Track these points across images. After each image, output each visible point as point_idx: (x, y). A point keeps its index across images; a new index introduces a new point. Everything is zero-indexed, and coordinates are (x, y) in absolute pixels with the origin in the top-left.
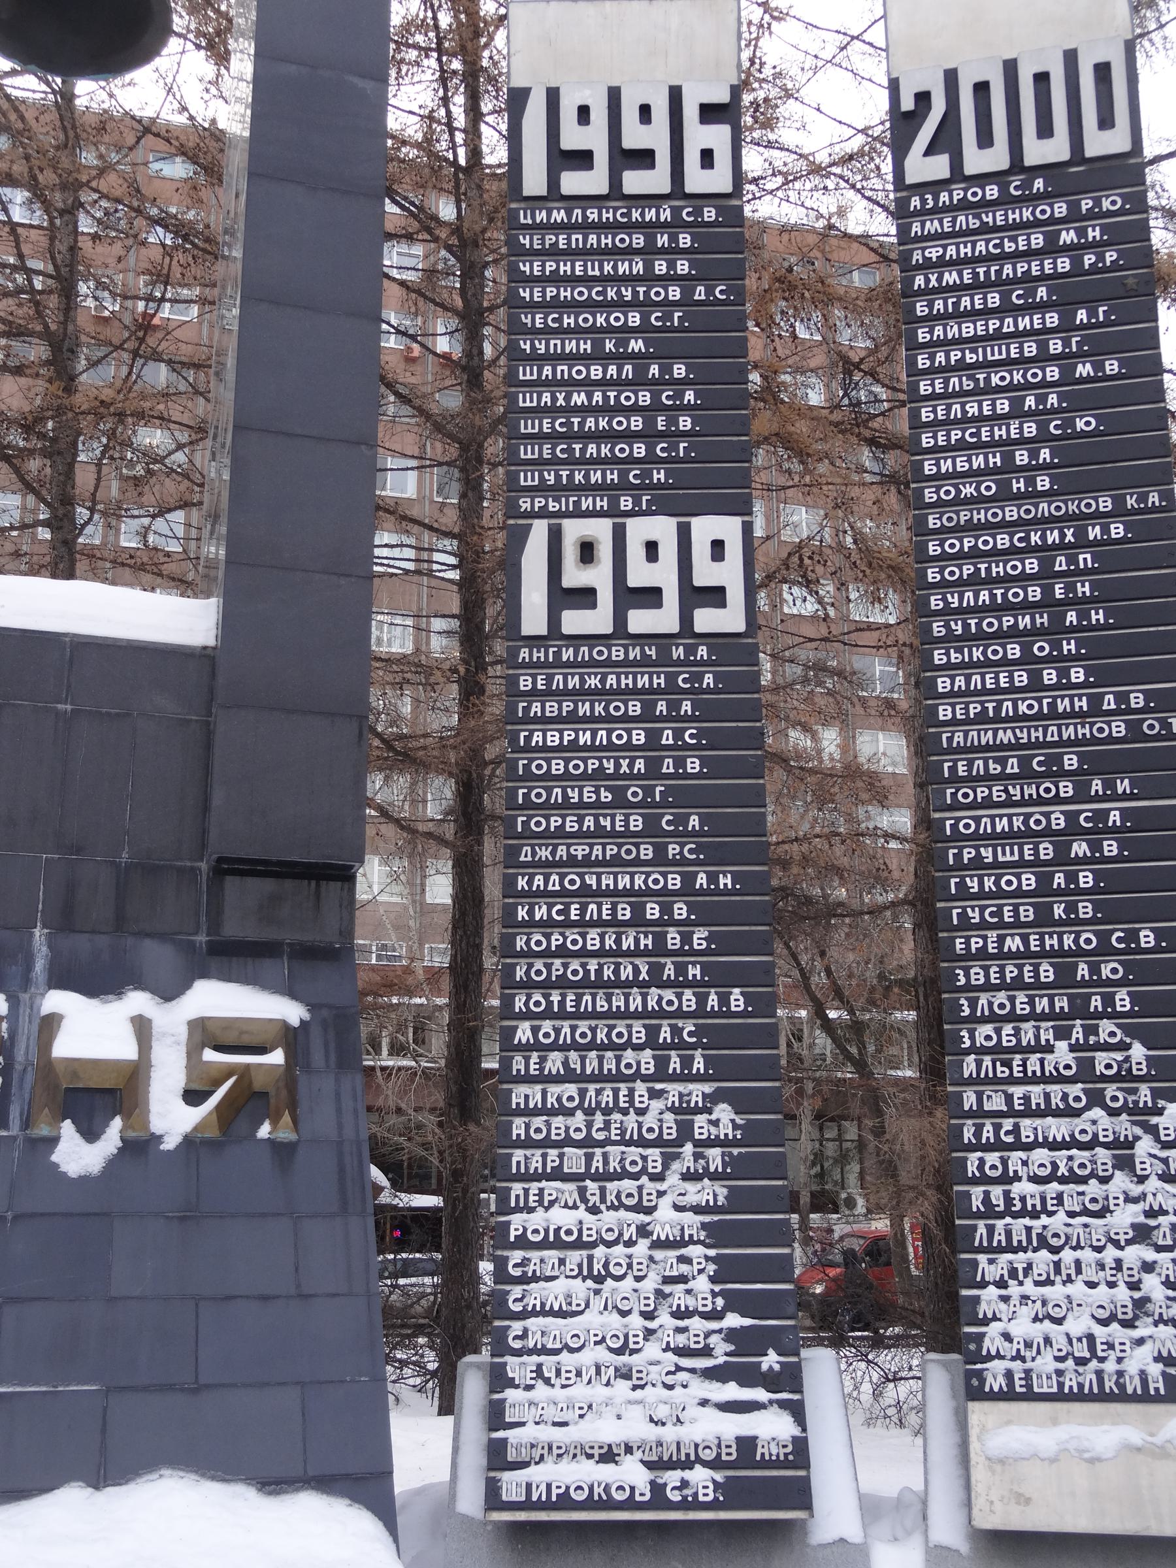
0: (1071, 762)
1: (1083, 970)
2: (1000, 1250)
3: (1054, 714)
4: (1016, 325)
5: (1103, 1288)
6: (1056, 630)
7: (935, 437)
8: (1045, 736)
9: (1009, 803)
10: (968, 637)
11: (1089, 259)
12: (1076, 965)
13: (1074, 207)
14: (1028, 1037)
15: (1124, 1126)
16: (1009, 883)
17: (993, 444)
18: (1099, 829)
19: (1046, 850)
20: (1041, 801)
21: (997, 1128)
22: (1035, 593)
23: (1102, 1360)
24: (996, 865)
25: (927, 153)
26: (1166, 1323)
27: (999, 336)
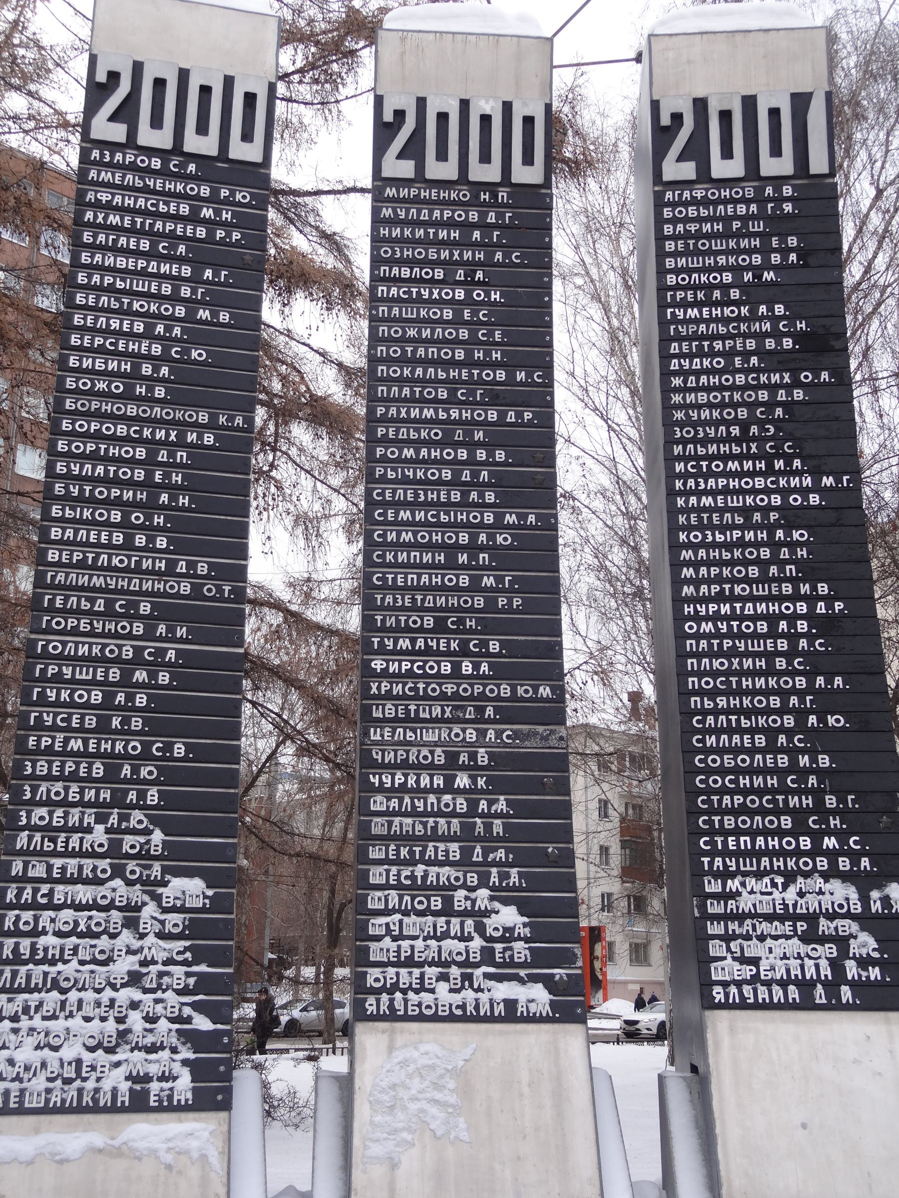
0: (145, 608)
1: (126, 770)
2: (20, 991)
3: (138, 570)
4: (159, 268)
5: (96, 1022)
6: (150, 506)
7: (82, 339)
8: (129, 585)
9: (92, 634)
10: (81, 500)
11: (220, 234)
12: (122, 765)
13: (215, 192)
14: (74, 818)
15: (136, 894)
16: (81, 697)
17: (126, 354)
18: (158, 663)
19: (115, 674)
20: (116, 636)
21: (35, 891)
22: (139, 475)
23: (85, 1080)
24: (73, 681)
25: (112, 119)
26: (140, 1050)
27: (143, 273)
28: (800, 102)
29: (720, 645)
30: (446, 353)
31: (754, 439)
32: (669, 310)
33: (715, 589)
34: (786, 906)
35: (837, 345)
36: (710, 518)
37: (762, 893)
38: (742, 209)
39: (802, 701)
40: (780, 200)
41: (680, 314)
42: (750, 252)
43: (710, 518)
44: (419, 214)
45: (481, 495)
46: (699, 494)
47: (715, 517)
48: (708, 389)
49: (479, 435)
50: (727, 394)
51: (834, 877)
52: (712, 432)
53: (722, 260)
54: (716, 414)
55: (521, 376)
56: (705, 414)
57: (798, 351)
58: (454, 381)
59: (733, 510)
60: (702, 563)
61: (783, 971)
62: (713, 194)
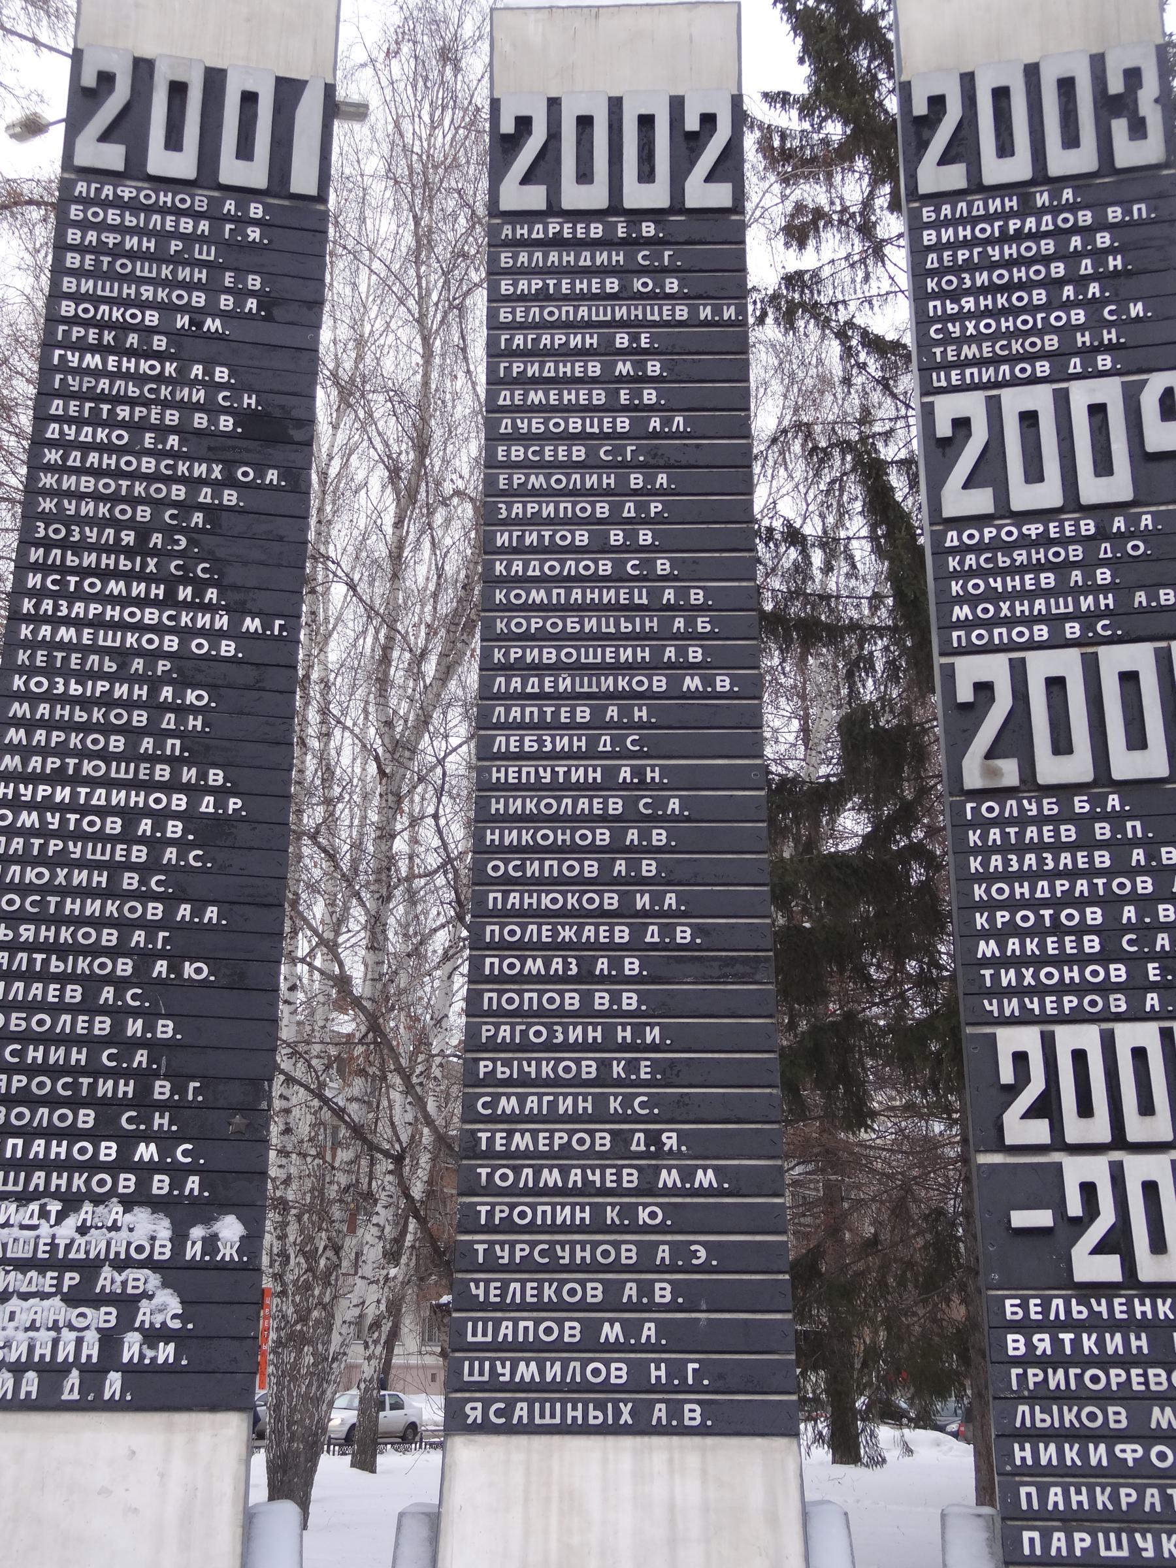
28: (288, 91)
31: (154, 553)
32: (57, 352)
33: (53, 763)
34: (53, 1246)
35: (297, 435)
36: (66, 659)
37: (23, 1227)
38: (186, 225)
39: (151, 938)
40: (244, 221)
41: (73, 359)
42: (189, 287)
43: (66, 659)
46: (56, 621)
47: (75, 659)
48: (97, 473)
50: (125, 483)
51: (141, 1204)
53: (147, 292)
54: (103, 510)
56: (87, 508)
57: (241, 437)
59: (103, 651)
61: (24, 1348)
62: (148, 195)
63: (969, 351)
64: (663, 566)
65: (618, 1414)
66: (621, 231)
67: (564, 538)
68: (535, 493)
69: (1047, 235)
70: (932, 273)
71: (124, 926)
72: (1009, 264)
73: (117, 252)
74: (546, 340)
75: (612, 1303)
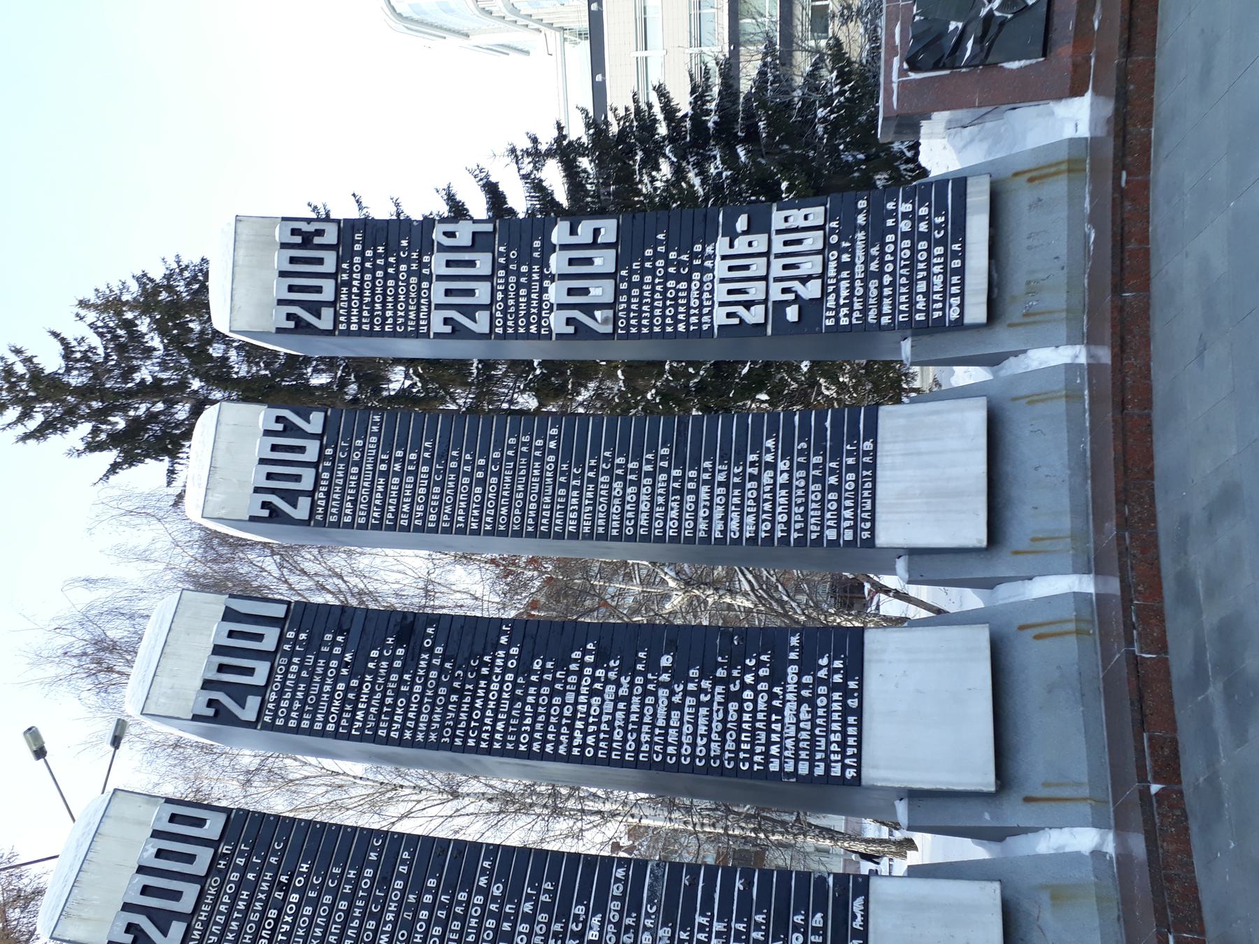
29: (605, 732)
30: (339, 917)
31: (463, 686)
33: (564, 730)
35: (410, 619)
36: (513, 726)
38: (294, 668)
42: (327, 667)
43: (513, 726)
44: (218, 924)
45: (459, 903)
46: (494, 731)
48: (419, 713)
49: (412, 898)
50: (426, 700)
52: (451, 715)
53: (327, 688)
54: (438, 710)
55: (373, 856)
56: (437, 718)
58: (363, 914)
59: (511, 708)
60: (544, 737)
62: (276, 687)
63: (412, 315)
64: (497, 455)
65: (867, 476)
66: (328, 464)
67: (476, 499)
68: (453, 511)
69: (362, 277)
70: (372, 328)
71: (645, 693)
72: (373, 294)
73: (304, 702)
74: (378, 502)
75: (821, 480)
